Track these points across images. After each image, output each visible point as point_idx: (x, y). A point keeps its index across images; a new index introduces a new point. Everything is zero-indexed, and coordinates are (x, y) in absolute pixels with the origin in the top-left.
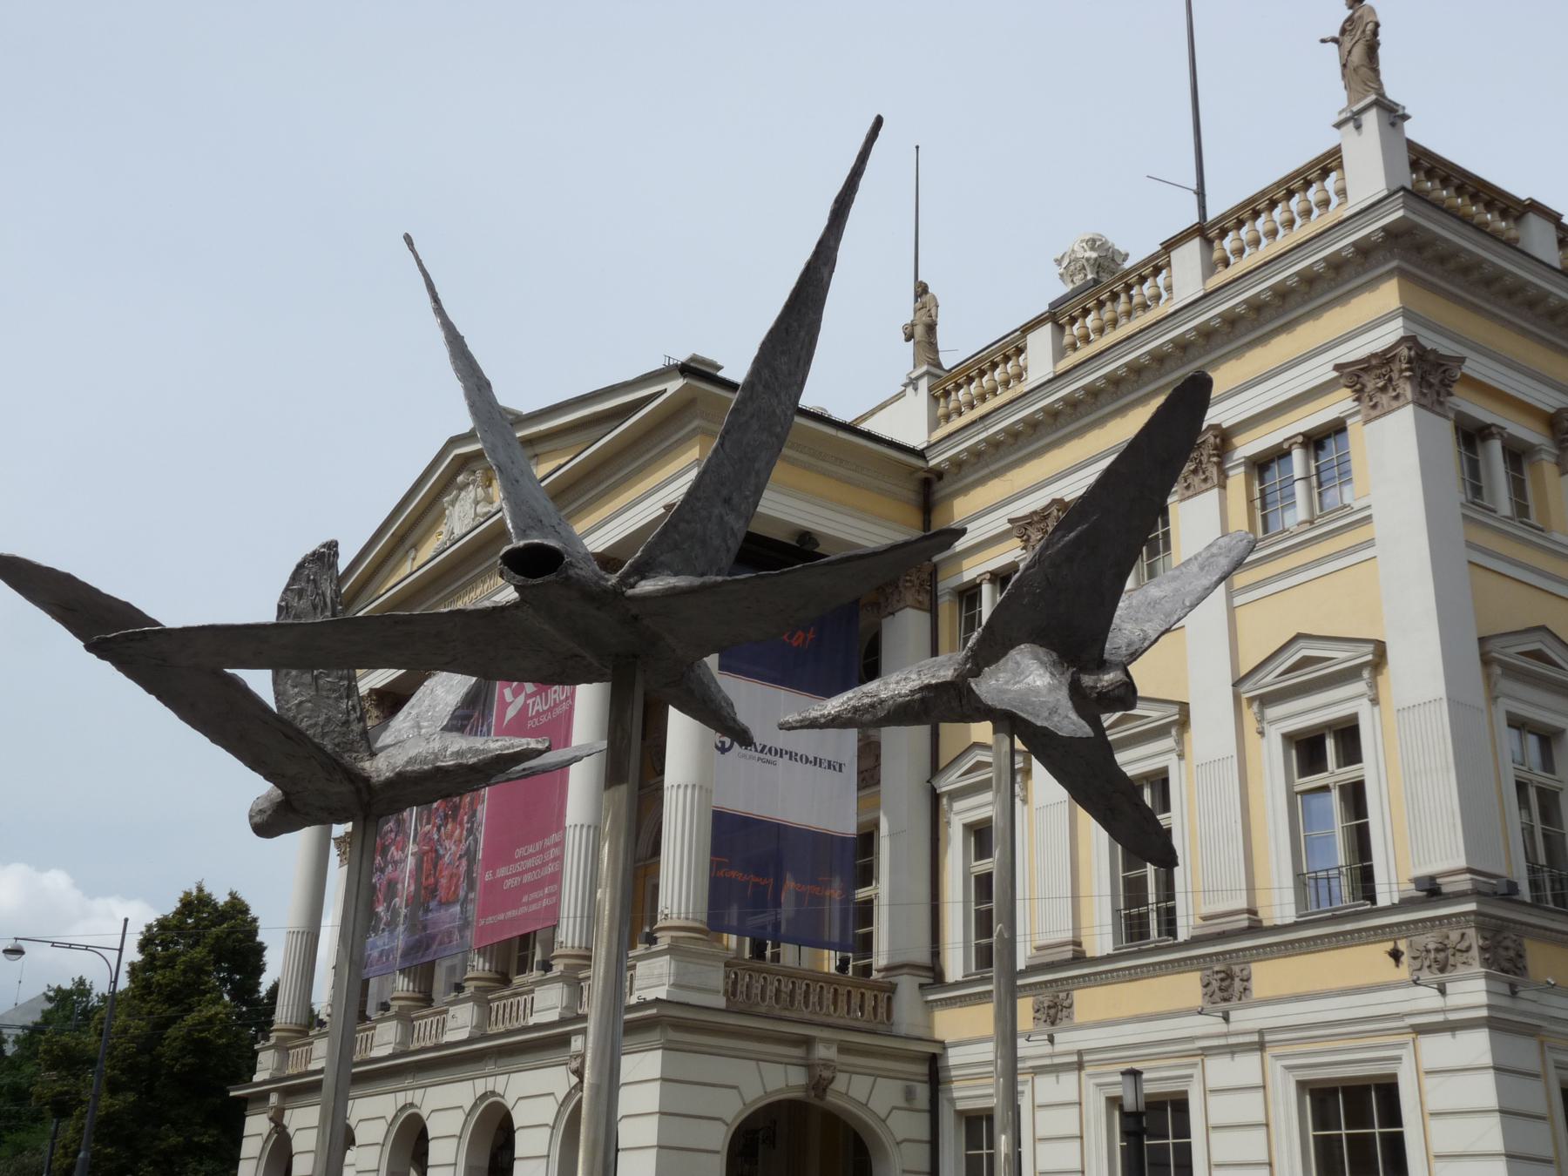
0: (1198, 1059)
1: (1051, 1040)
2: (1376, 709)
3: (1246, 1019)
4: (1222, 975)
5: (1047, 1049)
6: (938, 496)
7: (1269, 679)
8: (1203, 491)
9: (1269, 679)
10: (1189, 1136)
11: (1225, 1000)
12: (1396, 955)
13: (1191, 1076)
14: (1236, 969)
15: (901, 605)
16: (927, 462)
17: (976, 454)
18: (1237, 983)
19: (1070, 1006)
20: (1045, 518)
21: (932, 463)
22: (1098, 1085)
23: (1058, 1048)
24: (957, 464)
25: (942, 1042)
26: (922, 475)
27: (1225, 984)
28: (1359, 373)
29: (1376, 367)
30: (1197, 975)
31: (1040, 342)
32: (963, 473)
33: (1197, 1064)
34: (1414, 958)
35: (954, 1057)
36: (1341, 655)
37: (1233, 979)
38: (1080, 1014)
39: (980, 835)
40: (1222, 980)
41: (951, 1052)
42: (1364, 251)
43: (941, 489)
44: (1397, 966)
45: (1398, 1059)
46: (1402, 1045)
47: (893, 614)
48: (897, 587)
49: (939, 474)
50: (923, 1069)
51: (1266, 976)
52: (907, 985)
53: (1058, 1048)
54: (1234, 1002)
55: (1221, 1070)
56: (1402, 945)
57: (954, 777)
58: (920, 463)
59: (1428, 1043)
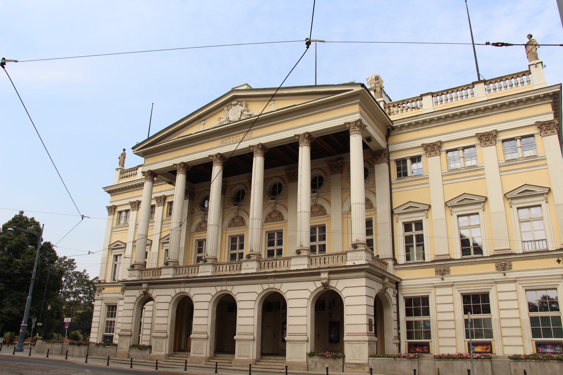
0: (494, 284)
1: (443, 279)
2: (547, 204)
4: (504, 264)
5: (441, 281)
6: (391, 134)
7: (515, 194)
8: (490, 146)
9: (515, 194)
10: (406, 308)
11: (504, 270)
13: (491, 288)
14: (507, 263)
15: (383, 161)
16: (393, 124)
17: (410, 125)
18: (507, 266)
19: (449, 271)
20: (434, 145)
21: (394, 125)
22: (458, 290)
23: (445, 281)
24: (402, 126)
25: (401, 279)
26: (389, 128)
27: (505, 266)
28: (542, 125)
29: (546, 124)
30: (494, 264)
31: (427, 100)
32: (402, 129)
33: (494, 285)
35: (404, 283)
36: (538, 190)
37: (506, 265)
38: (452, 273)
39: (407, 227)
40: (504, 265)
41: (403, 282)
43: (393, 133)
44: (559, 263)
47: (380, 163)
49: (393, 128)
51: (516, 265)
52: (390, 263)
53: (445, 281)
54: (507, 271)
55: (439, 291)
56: (560, 259)
57: (401, 210)
58: (392, 125)
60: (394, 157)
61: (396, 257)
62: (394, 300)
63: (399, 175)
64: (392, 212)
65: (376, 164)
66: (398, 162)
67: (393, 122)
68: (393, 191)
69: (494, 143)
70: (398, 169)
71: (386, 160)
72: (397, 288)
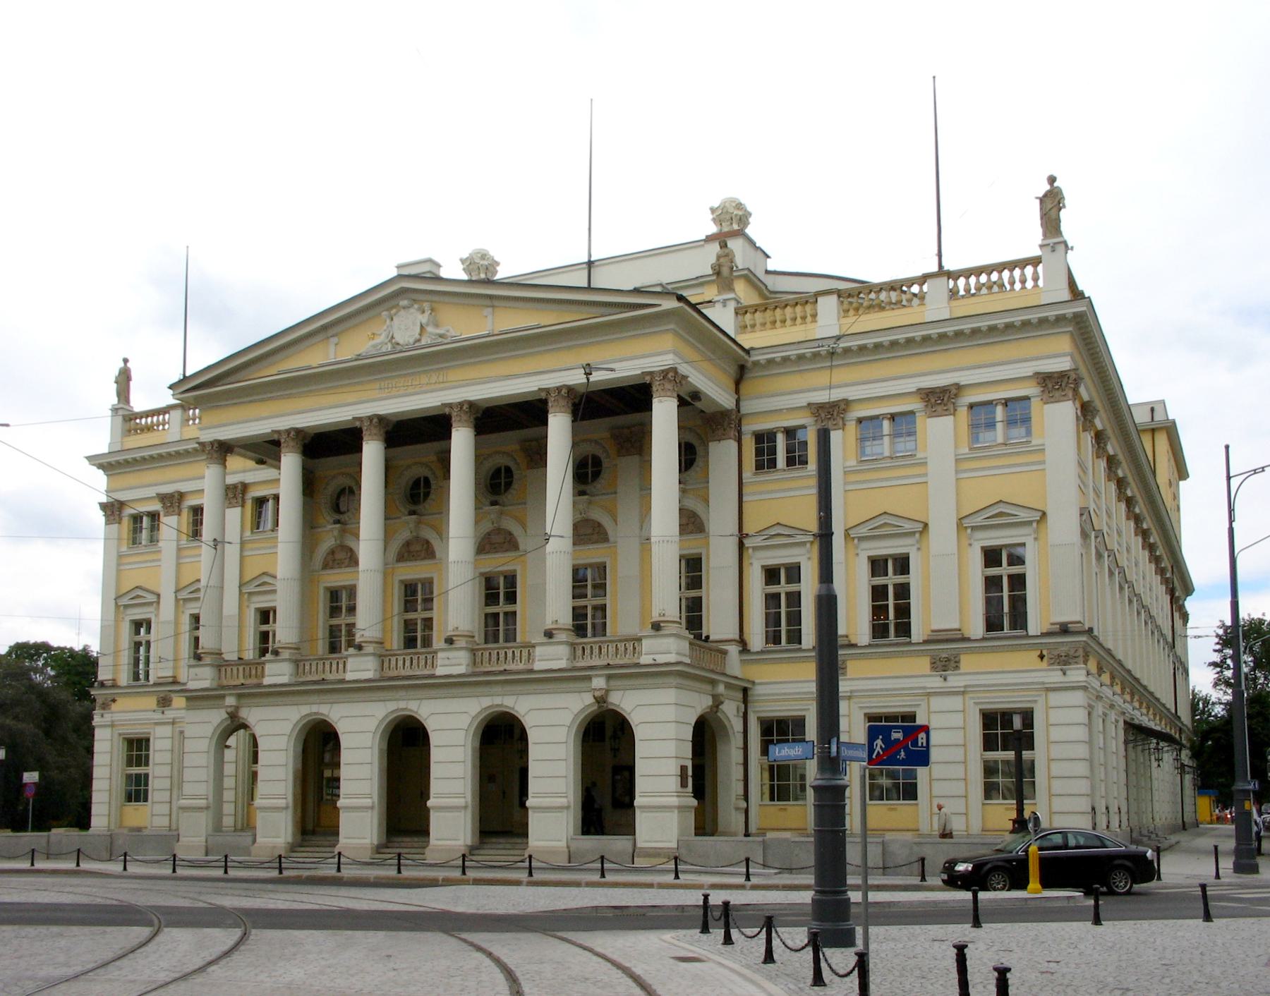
3: (955, 681)
12: (1042, 657)
20: (835, 406)
24: (771, 362)
34: (1051, 658)
35: (758, 690)
39: (771, 575)
41: (758, 687)
42: (1060, 319)
45: (1035, 701)
46: (1039, 696)
47: (719, 440)
48: (723, 426)
50: (740, 695)
52: (733, 650)
59: (1052, 695)
60: (750, 427)
61: (746, 637)
62: (737, 725)
63: (759, 466)
64: (741, 545)
65: (711, 441)
66: (760, 437)
67: (752, 352)
68: (745, 499)
69: (952, 411)
70: (759, 452)
71: (733, 433)
72: (745, 701)
